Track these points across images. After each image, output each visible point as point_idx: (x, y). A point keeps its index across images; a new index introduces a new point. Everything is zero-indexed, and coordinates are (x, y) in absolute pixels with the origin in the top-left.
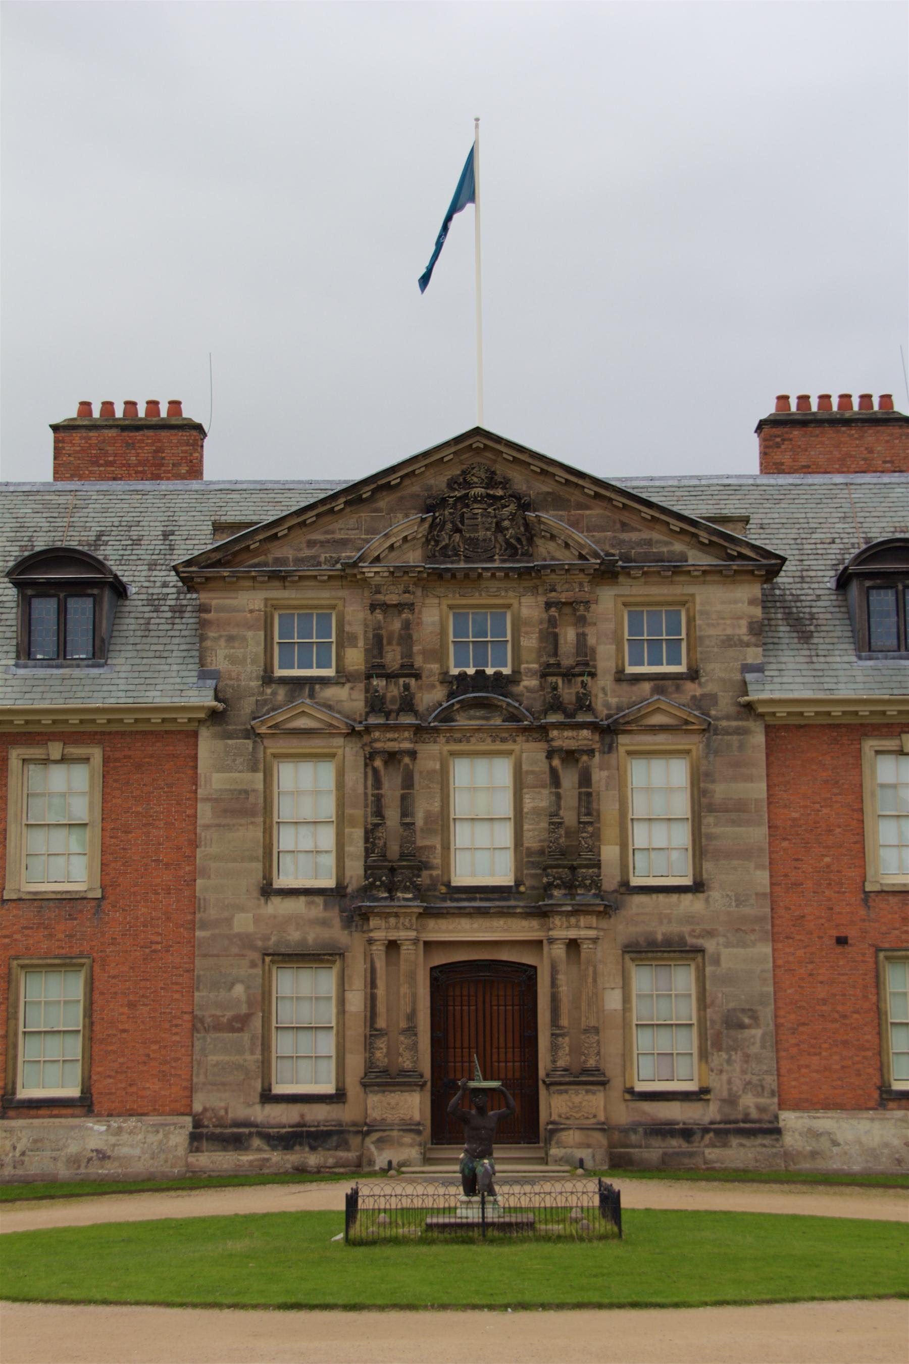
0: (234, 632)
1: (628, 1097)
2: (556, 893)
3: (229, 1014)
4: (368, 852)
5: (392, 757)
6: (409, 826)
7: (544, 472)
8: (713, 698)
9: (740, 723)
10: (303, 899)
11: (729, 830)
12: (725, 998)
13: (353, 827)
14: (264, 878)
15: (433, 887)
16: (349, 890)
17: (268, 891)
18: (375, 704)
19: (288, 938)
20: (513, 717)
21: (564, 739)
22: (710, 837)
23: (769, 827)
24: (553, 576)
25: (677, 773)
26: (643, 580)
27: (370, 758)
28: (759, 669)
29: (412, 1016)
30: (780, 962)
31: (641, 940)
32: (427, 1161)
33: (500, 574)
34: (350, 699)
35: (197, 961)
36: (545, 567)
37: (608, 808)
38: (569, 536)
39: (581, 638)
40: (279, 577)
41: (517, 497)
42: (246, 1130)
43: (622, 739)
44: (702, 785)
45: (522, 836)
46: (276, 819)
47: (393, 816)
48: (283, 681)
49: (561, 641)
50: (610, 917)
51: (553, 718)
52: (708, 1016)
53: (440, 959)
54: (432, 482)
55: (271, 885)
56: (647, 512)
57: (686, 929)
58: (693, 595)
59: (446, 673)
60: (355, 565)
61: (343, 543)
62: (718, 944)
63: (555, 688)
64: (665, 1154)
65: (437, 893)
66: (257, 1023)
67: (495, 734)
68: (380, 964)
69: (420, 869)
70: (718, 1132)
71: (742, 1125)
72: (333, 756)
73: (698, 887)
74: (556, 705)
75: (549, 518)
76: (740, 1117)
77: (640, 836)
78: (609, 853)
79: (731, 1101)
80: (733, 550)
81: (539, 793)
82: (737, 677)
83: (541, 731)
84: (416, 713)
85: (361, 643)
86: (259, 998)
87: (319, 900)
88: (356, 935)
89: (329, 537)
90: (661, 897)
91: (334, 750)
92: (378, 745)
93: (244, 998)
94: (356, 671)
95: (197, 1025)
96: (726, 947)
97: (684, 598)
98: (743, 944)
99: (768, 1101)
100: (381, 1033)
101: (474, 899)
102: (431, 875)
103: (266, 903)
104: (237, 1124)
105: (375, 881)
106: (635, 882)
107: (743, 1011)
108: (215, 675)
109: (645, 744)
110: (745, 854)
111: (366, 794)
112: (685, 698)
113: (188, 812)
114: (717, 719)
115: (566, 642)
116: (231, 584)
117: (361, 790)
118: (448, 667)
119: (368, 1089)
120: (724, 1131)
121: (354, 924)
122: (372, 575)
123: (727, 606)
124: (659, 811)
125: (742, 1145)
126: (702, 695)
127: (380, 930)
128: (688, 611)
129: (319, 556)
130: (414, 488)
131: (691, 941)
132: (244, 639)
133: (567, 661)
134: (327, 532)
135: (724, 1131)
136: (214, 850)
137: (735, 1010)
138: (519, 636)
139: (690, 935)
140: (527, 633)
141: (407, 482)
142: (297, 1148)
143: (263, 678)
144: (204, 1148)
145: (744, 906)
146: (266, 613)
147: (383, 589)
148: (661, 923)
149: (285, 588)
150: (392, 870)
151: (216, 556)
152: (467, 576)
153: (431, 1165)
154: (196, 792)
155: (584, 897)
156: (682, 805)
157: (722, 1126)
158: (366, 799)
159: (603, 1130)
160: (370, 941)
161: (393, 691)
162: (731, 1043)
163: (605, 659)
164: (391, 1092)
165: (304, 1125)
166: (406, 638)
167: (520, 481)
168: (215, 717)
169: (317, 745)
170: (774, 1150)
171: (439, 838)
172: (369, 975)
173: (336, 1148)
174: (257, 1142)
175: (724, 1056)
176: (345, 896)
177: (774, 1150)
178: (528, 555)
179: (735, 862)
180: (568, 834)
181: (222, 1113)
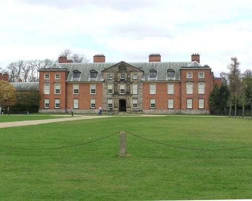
12: (139, 102)
25: (136, 86)
34: (113, 80)
38: (129, 69)
75: (127, 68)
78: (131, 92)
95: (103, 103)
120: (139, 111)
123: (141, 74)
135: (139, 111)
163: (131, 78)
168: (104, 81)
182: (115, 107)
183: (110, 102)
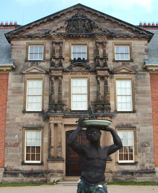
0: (18, 50)
1: (117, 164)
2: (99, 111)
3: (14, 143)
4: (50, 101)
5: (56, 78)
6: (60, 94)
7: (95, 14)
8: (137, 66)
9: (144, 72)
10: (33, 114)
11: (142, 98)
12: (141, 139)
13: (46, 96)
14: (24, 109)
15: (67, 110)
16: (45, 112)
17: (24, 112)
18: (52, 64)
19: (30, 124)
20: (88, 68)
21: (100, 73)
22: (137, 99)
23: (152, 98)
24: (97, 36)
26: (119, 39)
27: (51, 78)
28: (148, 60)
29: (60, 143)
30: (155, 131)
31: (120, 125)
32: (64, 180)
33: (85, 36)
34: (46, 65)
35: (6, 129)
36: (95, 33)
37: (111, 91)
39: (104, 51)
40: (30, 37)
41: (89, 20)
42: (18, 172)
43: (115, 75)
44: (135, 87)
45: (90, 98)
46: (27, 95)
47: (56, 93)
48: (30, 61)
49: (99, 52)
50: (112, 119)
51: (98, 68)
52: (137, 144)
53: (68, 129)
54: (68, 17)
55: (25, 110)
56: (120, 23)
57: (131, 122)
58: (131, 43)
59: (71, 59)
60: (48, 33)
61: (46, 30)
62: (139, 126)
63: (98, 61)
64: (126, 178)
65: (67, 112)
66: (21, 145)
67: (82, 72)
68: (52, 129)
69: (63, 106)
70: (140, 173)
71: (145, 171)
72: (41, 79)
73: (134, 112)
74: (98, 65)
76: (145, 169)
77: (119, 99)
78: (112, 103)
79: (143, 165)
80: (141, 32)
81: (94, 87)
82: (143, 62)
83: (94, 72)
84: (63, 67)
85: (50, 53)
86: (22, 139)
87: (37, 114)
88: (47, 123)
89: (43, 29)
90: (125, 114)
91: (42, 78)
92: (53, 74)
93: (18, 139)
94: (48, 59)
95: (6, 145)
96: (141, 126)
97: (129, 43)
98: (146, 126)
99: (152, 165)
100: (52, 147)
101: (78, 114)
102: (66, 107)
103: (24, 115)
104: (15, 170)
105: (51, 108)
106: (118, 110)
107: (146, 142)
108: (14, 60)
109: (121, 77)
110: (146, 104)
111: (50, 87)
112: (130, 66)
113: (6, 93)
114: (138, 71)
115: (101, 52)
116: (18, 39)
117: (48, 87)
118: (71, 58)
119: (49, 162)
120: (141, 172)
121: (46, 120)
122: (53, 35)
124: (124, 93)
125: (145, 176)
126: (134, 66)
127: (53, 121)
128: (130, 46)
129: (40, 33)
130: (64, 18)
131: (132, 125)
132: (21, 52)
133: (101, 57)
134: (42, 28)
135: (141, 172)
136: (11, 102)
137: (144, 142)
138: (89, 51)
139: (132, 124)
140: (91, 50)
141: (62, 16)
142: (31, 177)
143: (25, 60)
144: (7, 176)
145: (146, 116)
146: (27, 46)
147: (55, 39)
148: (125, 120)
149: (31, 40)
150: (56, 105)
151: (15, 32)
152: (76, 37)
153: (65, 181)
154: (8, 88)
155: (106, 112)
156: (129, 92)
157: (141, 171)
158: (50, 89)
159: (112, 173)
160: (50, 124)
161: (57, 62)
162: (143, 150)
163: (110, 57)
164: (55, 162)
165: (33, 171)
166: (60, 51)
167: (89, 16)
168: (13, 69)
169: (38, 76)
170: (154, 177)
171: (68, 98)
172: (49, 133)
173: (41, 177)
174: (20, 175)
175: (141, 154)
176: (44, 113)
177: (154, 177)
178: (91, 32)
179: (143, 106)
180: (102, 97)
181: (12, 167)
182: (53, 159)
183: (32, 138)
